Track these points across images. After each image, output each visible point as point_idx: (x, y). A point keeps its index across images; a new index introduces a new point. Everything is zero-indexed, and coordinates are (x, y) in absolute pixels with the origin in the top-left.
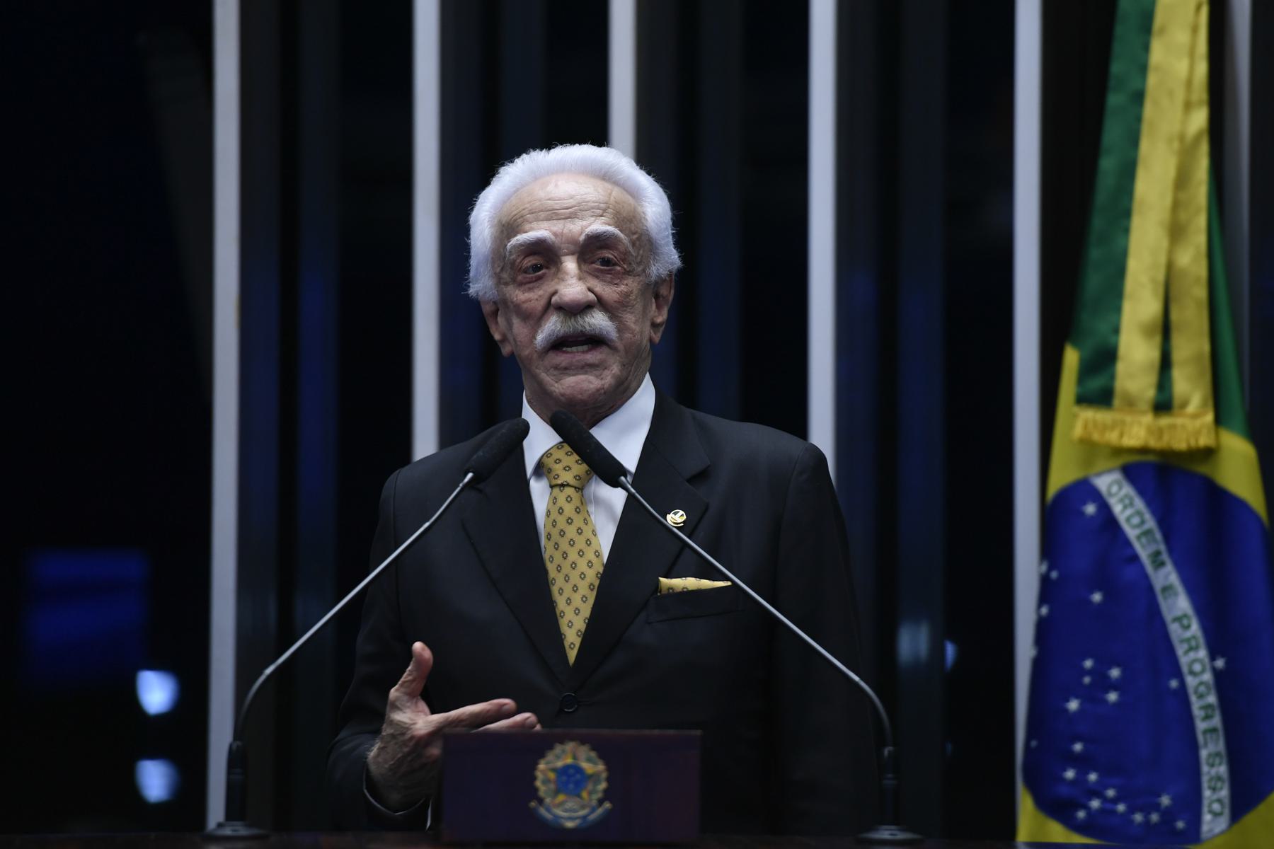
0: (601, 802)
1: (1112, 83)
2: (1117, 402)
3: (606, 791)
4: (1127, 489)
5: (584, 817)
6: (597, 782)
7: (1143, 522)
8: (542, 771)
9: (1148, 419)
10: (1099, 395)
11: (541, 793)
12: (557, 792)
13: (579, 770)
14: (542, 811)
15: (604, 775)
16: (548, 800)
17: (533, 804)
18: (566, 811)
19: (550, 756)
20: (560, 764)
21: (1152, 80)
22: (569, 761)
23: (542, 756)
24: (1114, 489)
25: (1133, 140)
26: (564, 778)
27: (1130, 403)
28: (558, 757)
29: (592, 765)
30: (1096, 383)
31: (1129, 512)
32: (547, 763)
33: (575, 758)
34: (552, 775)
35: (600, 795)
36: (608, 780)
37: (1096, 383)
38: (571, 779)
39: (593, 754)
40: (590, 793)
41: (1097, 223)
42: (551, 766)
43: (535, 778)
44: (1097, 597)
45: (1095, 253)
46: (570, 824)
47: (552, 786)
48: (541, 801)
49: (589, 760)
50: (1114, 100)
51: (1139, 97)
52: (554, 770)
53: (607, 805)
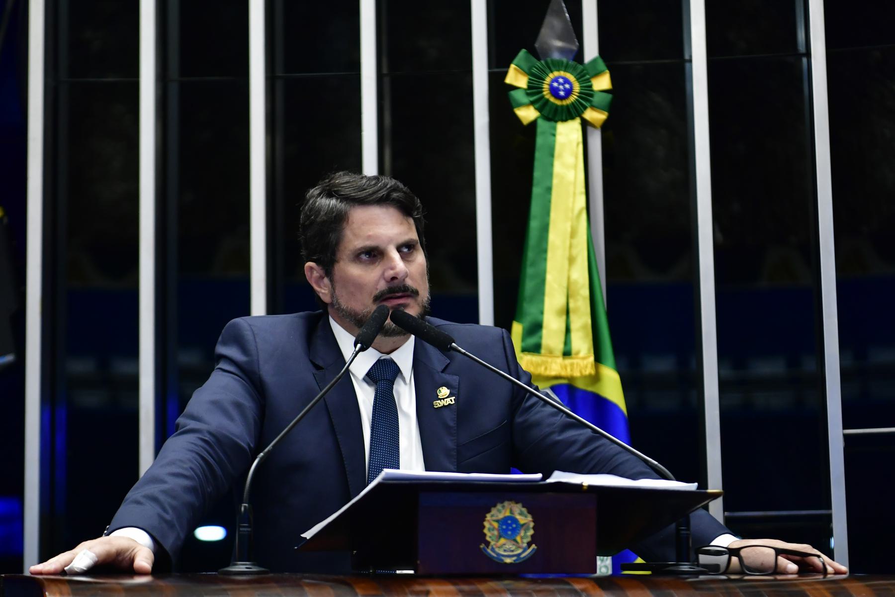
0: (529, 544)
1: (535, 181)
2: (543, 351)
3: (532, 536)
5: (519, 555)
6: (527, 530)
9: (560, 360)
10: (536, 349)
11: (488, 539)
12: (500, 537)
13: (515, 521)
14: (489, 551)
15: (532, 524)
16: (492, 543)
17: (482, 546)
20: (501, 516)
21: (555, 181)
22: (508, 514)
23: (489, 511)
26: (504, 527)
27: (551, 352)
28: (499, 511)
29: (525, 519)
30: (532, 341)
32: (492, 516)
33: (511, 512)
34: (496, 525)
35: (529, 539)
36: (534, 528)
37: (532, 341)
38: (509, 527)
39: (524, 510)
40: (522, 538)
41: (531, 254)
42: (494, 518)
43: (484, 527)
45: (530, 271)
46: (508, 561)
47: (496, 533)
48: (488, 544)
49: (521, 514)
50: (536, 191)
51: (549, 190)
52: (497, 521)
53: (534, 546)
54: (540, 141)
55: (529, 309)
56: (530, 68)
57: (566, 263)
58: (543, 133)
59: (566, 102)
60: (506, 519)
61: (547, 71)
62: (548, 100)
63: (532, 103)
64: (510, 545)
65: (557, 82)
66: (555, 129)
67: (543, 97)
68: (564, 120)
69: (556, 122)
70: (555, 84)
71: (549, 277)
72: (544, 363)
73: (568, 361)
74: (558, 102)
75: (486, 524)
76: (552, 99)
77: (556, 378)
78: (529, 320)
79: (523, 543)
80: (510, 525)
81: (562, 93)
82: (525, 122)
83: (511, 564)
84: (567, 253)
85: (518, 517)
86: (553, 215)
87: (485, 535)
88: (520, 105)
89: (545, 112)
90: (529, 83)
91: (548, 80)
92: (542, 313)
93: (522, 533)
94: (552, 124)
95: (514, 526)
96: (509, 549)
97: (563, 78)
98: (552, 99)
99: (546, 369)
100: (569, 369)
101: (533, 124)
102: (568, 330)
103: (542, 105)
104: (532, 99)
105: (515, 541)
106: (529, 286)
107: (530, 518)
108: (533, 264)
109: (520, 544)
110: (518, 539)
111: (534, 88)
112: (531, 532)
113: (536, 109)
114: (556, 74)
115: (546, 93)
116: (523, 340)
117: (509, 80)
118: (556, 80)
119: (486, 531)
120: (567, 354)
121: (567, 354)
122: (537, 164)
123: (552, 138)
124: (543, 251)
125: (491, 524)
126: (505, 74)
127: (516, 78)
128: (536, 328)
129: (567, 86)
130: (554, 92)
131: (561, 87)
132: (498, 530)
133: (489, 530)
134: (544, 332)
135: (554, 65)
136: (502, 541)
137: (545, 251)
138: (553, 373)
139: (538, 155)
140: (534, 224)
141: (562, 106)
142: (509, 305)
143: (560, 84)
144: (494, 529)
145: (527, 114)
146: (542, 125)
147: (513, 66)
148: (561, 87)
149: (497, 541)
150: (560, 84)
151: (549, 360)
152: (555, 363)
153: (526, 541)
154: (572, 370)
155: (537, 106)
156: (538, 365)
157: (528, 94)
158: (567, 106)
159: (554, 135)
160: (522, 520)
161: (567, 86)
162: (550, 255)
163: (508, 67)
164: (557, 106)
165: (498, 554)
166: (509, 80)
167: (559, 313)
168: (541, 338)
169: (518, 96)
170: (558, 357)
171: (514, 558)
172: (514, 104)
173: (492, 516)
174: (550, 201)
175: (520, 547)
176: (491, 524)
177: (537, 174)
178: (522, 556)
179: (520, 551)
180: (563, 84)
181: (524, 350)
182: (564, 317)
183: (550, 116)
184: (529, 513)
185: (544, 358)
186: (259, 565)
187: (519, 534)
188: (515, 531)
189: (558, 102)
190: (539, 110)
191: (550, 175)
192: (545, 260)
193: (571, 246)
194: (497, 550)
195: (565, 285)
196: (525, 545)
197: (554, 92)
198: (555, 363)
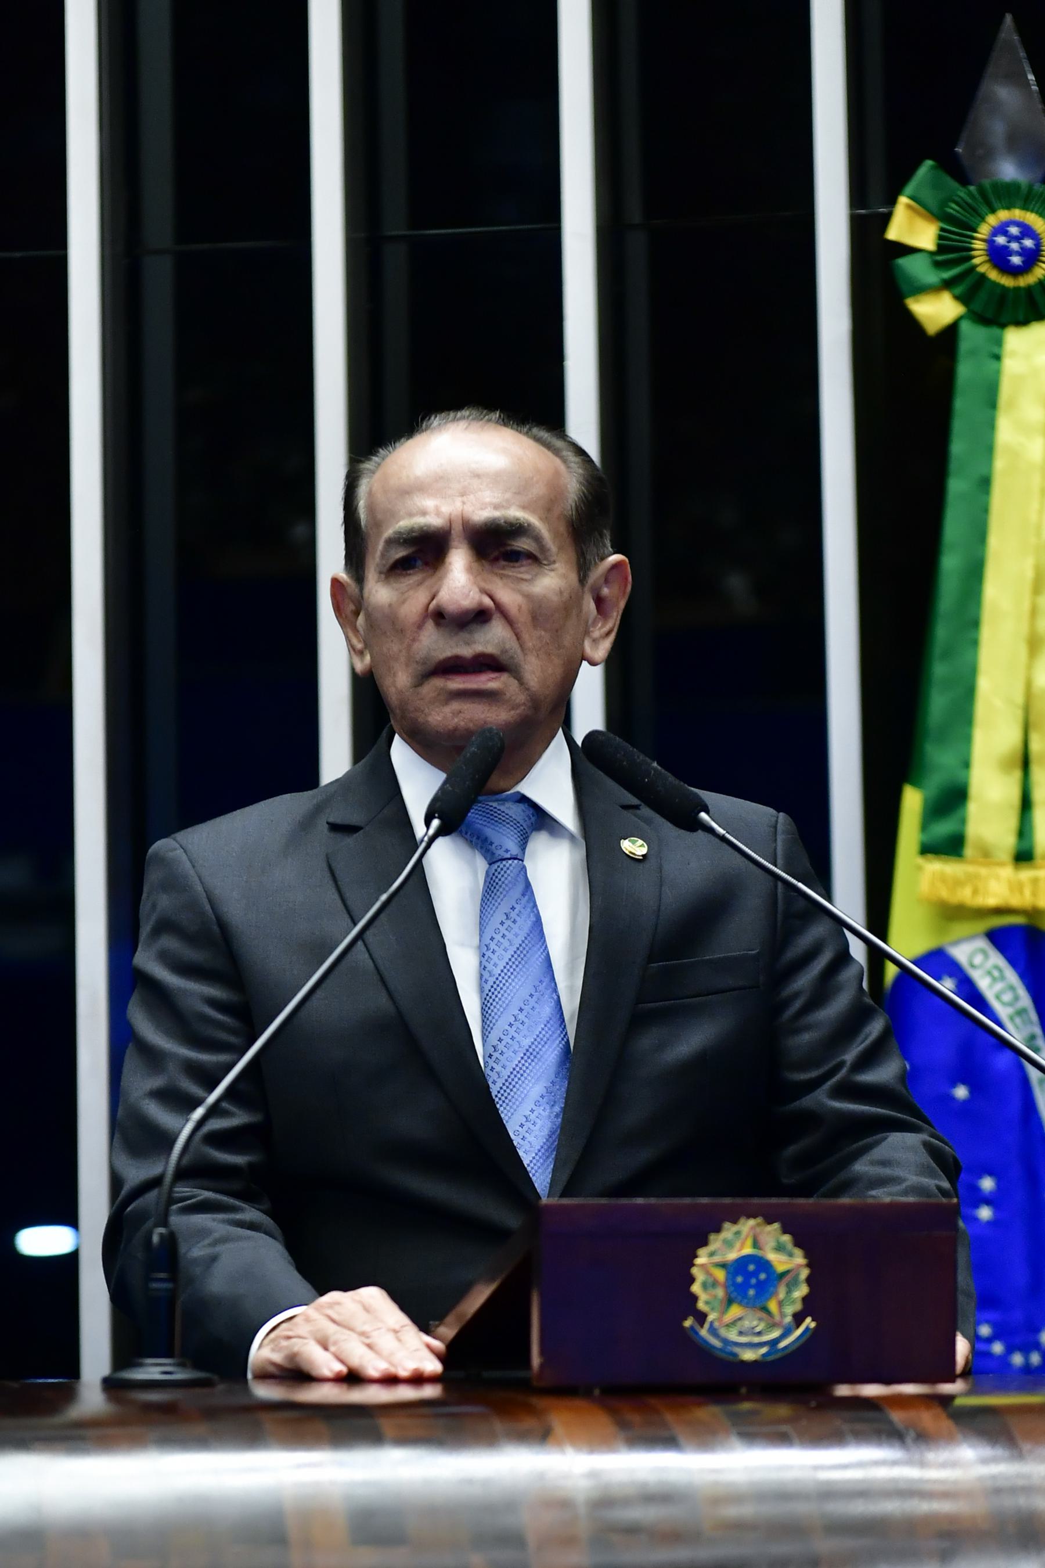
0: (798, 1319)
1: (953, 465)
2: (969, 851)
3: (805, 1299)
4: (997, 959)
5: (774, 1342)
6: (791, 1286)
7: (1016, 998)
8: (703, 1266)
10: (951, 846)
11: (701, 1305)
12: (730, 1301)
13: (763, 1265)
14: (704, 1332)
15: (805, 1273)
17: (688, 1323)
18: (741, 1333)
19: (716, 1242)
20: (732, 1256)
21: (1000, 464)
22: (748, 1250)
23: (705, 1243)
24: (978, 960)
25: (980, 534)
26: (739, 1279)
27: (986, 854)
28: (729, 1244)
29: (787, 1258)
30: (943, 828)
31: (999, 986)
32: (712, 1254)
33: (756, 1244)
34: (720, 1275)
35: (798, 1307)
36: (809, 1281)
37: (943, 828)
38: (751, 1279)
39: (787, 1238)
40: (780, 1304)
41: (942, 632)
42: (717, 1259)
44: (961, 1092)
45: (939, 670)
46: (748, 1355)
47: (720, 1293)
48: (701, 1317)
49: (780, 1248)
50: (956, 486)
51: (985, 483)
52: (723, 1266)
53: (809, 1323)
54: (964, 370)
55: (938, 758)
56: (944, 203)
57: (1023, 651)
58: (973, 353)
59: (1026, 281)
60: (742, 1263)
61: (984, 209)
62: (983, 277)
63: (947, 285)
64: (753, 1321)
65: (1005, 233)
66: (999, 342)
67: (974, 268)
68: (1022, 322)
69: (1003, 326)
70: (1001, 240)
71: (985, 684)
72: (971, 878)
73: (1026, 874)
74: (1007, 281)
75: (695, 1271)
76: (994, 275)
77: (999, 911)
78: (936, 781)
79: (783, 1315)
80: (755, 1274)
81: (1016, 260)
82: (932, 327)
83: (755, 1363)
84: (1024, 629)
85: (772, 1256)
86: (995, 541)
87: (695, 1298)
88: (922, 290)
89: (977, 306)
90: (940, 238)
91: (984, 230)
92: (967, 764)
93: (782, 1293)
94: (995, 330)
95: (763, 1276)
96: (746, 1332)
97: (1018, 224)
98: (994, 275)
99: (975, 892)
100: (1027, 892)
101: (951, 331)
102: (1026, 804)
103: (969, 288)
104: (947, 275)
105: (765, 1309)
106: (937, 704)
107: (799, 1259)
108: (948, 654)
109: (777, 1318)
110: (773, 1306)
111: (951, 251)
112: (803, 1290)
113: (957, 298)
114: (1003, 215)
115: (980, 260)
116: (925, 825)
117: (894, 233)
118: (1001, 229)
119: (696, 1288)
120: (1024, 856)
121: (1024, 856)
122: (959, 426)
123: (993, 364)
124: (970, 623)
125: (708, 1273)
126: (886, 220)
127: (911, 227)
128: (952, 799)
129: (1028, 243)
130: (998, 257)
131: (1014, 246)
132: (726, 1287)
133: (705, 1286)
134: (973, 808)
135: (999, 198)
136: (735, 1311)
137: (975, 624)
138: (992, 901)
139: (960, 404)
140: (950, 563)
141: (1017, 289)
142: (895, 749)
143: (1012, 238)
144: (715, 1283)
145: (936, 310)
146: (971, 335)
147: (903, 200)
148: (1014, 246)
149: (724, 1312)
150: (1012, 238)
151: (983, 871)
152: (998, 878)
153: (790, 1310)
154: (1034, 894)
155: (959, 290)
156: (957, 883)
157: (938, 265)
158: (1029, 289)
159: (998, 358)
160: (779, 1262)
161: (1028, 243)
162: (987, 633)
163: (892, 202)
164: (1004, 289)
165: (726, 1342)
166: (894, 233)
167: (1005, 766)
168: (963, 821)
169: (915, 268)
170: (1001, 864)
171: (764, 1350)
172: (904, 288)
173: (712, 1254)
174: (985, 510)
175: (773, 1325)
176: (708, 1273)
177: (957, 447)
178: (782, 1344)
179: (775, 1334)
180: (1017, 239)
181: (928, 850)
182: (1018, 774)
183: (989, 315)
184: (797, 1244)
185: (970, 869)
186: (197, 1366)
187: (775, 1293)
188: (765, 1289)
189: (1007, 281)
190: (962, 299)
191: (987, 449)
192: (975, 643)
193: (1034, 612)
194: (723, 1332)
195: (1020, 699)
196: (789, 1319)
197: (998, 257)
198: (998, 878)
